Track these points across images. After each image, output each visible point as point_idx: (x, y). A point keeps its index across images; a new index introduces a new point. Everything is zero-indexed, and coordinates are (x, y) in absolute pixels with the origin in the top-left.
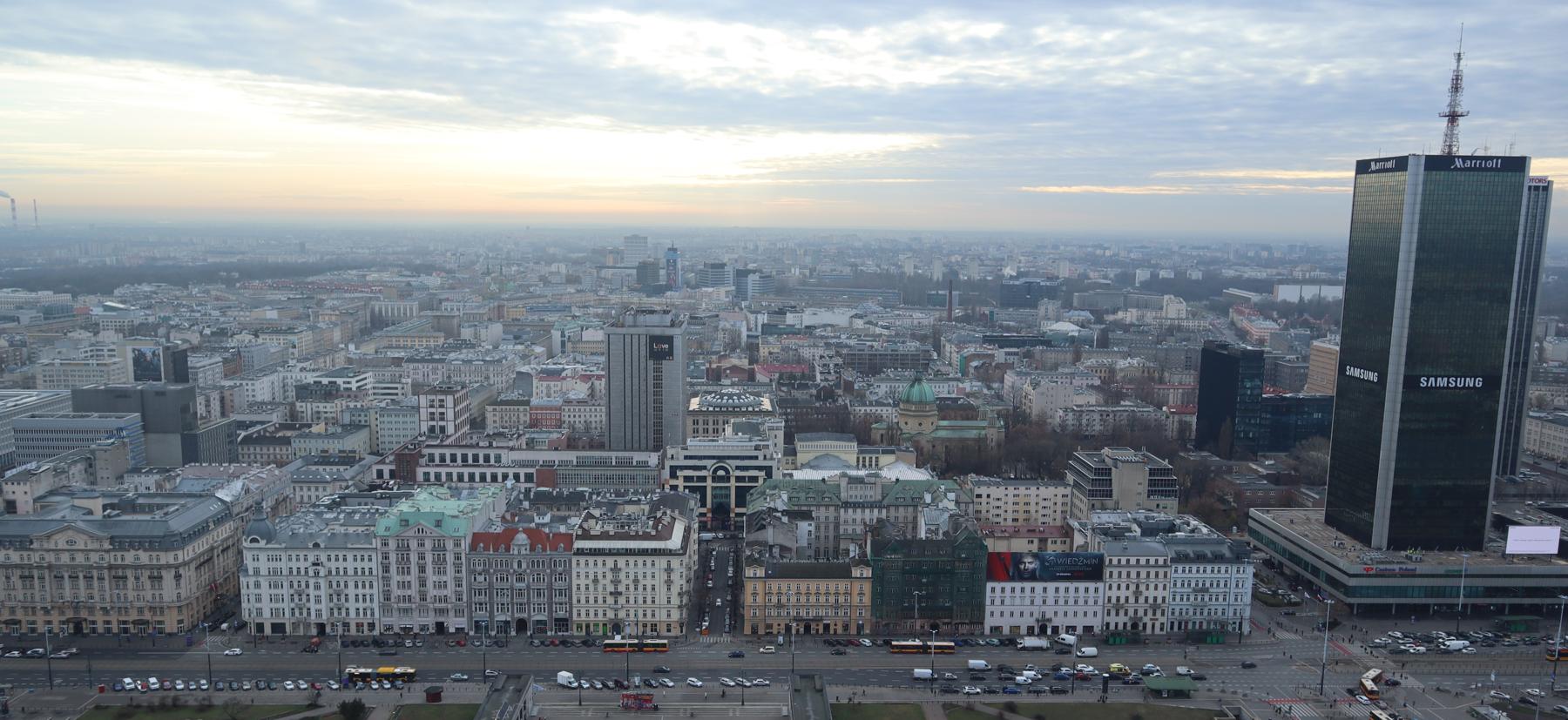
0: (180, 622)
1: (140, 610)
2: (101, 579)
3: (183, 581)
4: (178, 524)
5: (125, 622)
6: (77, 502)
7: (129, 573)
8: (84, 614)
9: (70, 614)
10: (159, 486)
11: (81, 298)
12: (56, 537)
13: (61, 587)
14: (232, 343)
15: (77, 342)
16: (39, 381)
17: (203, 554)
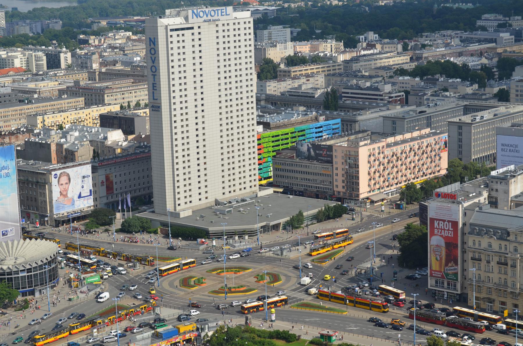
16: (512, 96)
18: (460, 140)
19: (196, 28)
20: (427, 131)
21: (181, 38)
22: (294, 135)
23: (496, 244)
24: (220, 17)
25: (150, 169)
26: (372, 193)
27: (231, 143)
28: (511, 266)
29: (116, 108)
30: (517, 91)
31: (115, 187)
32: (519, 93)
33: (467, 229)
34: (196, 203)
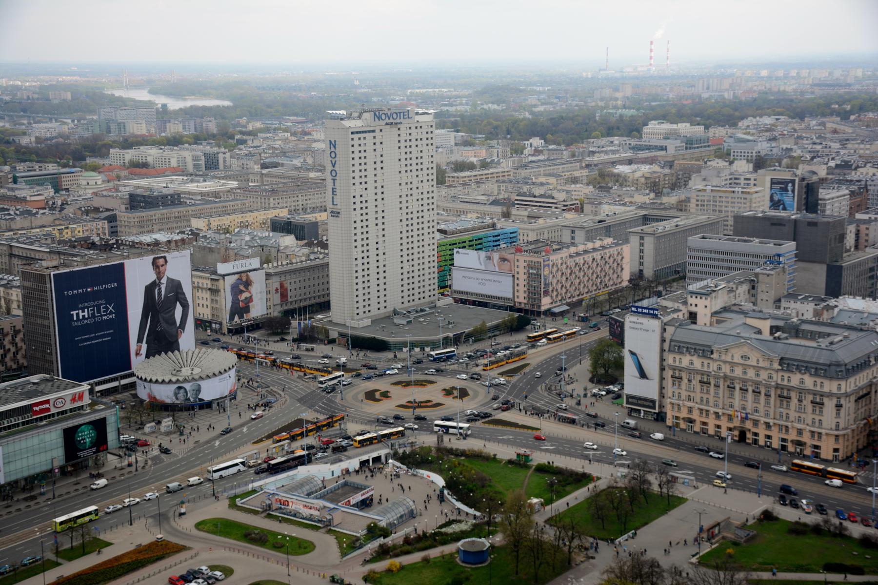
0: (836, 450)
1: (800, 432)
2: (768, 395)
3: (843, 411)
4: (846, 355)
5: (784, 440)
6: (749, 321)
7: (793, 395)
8: (748, 425)
9: (737, 423)
10: (817, 313)
11: (712, 130)
12: (733, 351)
13: (732, 396)
14: (854, 176)
15: (719, 171)
16: (692, 205)
17: (861, 388)
18: (641, 251)
19: (378, 131)
20: (609, 240)
21: (362, 142)
22: (471, 243)
23: (698, 363)
24: (402, 120)
25: (328, 276)
26: (554, 305)
27: (411, 251)
28: (766, 395)
29: (283, 214)
30: (697, 201)
31: (289, 294)
32: (699, 203)
33: (666, 346)
34: (374, 312)
